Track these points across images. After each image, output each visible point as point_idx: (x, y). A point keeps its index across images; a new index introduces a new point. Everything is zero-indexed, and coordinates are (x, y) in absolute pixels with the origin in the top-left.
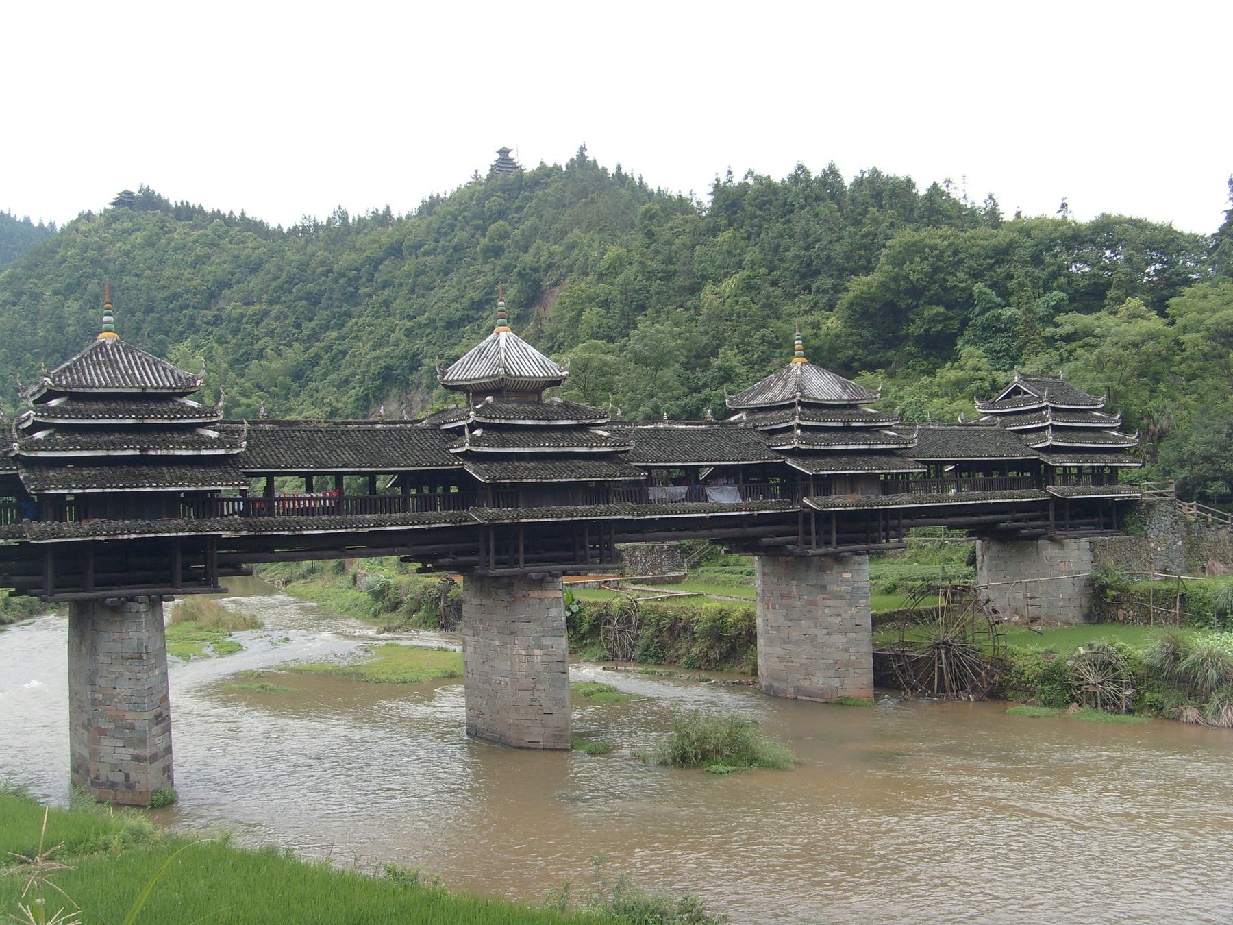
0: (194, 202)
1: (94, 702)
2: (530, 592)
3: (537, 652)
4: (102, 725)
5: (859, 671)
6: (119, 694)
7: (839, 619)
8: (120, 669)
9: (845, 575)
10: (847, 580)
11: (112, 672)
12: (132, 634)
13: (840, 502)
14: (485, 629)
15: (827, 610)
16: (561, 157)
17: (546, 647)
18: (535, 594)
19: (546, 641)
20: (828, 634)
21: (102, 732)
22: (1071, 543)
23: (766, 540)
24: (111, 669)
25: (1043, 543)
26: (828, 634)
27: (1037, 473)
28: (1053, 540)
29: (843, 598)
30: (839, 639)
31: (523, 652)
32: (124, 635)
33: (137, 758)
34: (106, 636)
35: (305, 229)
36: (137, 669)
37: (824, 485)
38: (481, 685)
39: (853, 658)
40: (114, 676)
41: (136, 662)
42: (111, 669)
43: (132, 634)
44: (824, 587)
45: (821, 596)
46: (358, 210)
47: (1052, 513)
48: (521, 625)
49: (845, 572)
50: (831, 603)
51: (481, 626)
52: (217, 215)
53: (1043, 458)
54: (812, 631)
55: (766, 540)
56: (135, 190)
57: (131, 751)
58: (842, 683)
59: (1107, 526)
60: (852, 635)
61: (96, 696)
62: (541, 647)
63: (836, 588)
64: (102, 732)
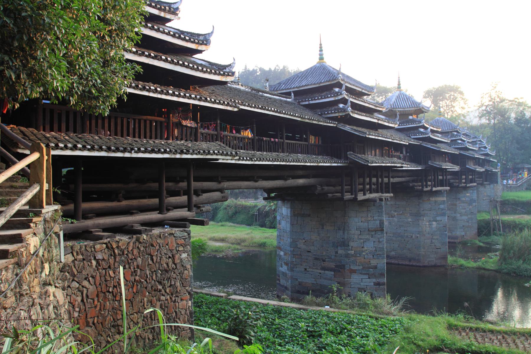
1: (347, 256)
2: (431, 198)
3: (434, 223)
4: (352, 267)
5: (472, 229)
6: (366, 250)
7: (465, 210)
8: (368, 237)
9: (467, 194)
10: (468, 196)
11: (361, 239)
12: (376, 218)
14: (401, 214)
15: (461, 207)
17: (439, 221)
18: (433, 199)
19: (438, 218)
20: (460, 216)
21: (354, 271)
22: (488, 187)
24: (360, 237)
26: (460, 216)
29: (467, 203)
30: (465, 218)
31: (428, 223)
32: (370, 219)
33: (378, 284)
34: (356, 220)
36: (379, 236)
38: (394, 239)
39: (470, 224)
40: (362, 241)
41: (379, 233)
42: (360, 237)
43: (376, 218)
44: (459, 199)
45: (458, 202)
48: (426, 212)
49: (468, 193)
50: (462, 204)
51: (396, 214)
54: (453, 215)
57: (374, 280)
58: (466, 234)
60: (470, 216)
61: (349, 252)
62: (436, 221)
63: (464, 199)
64: (354, 271)
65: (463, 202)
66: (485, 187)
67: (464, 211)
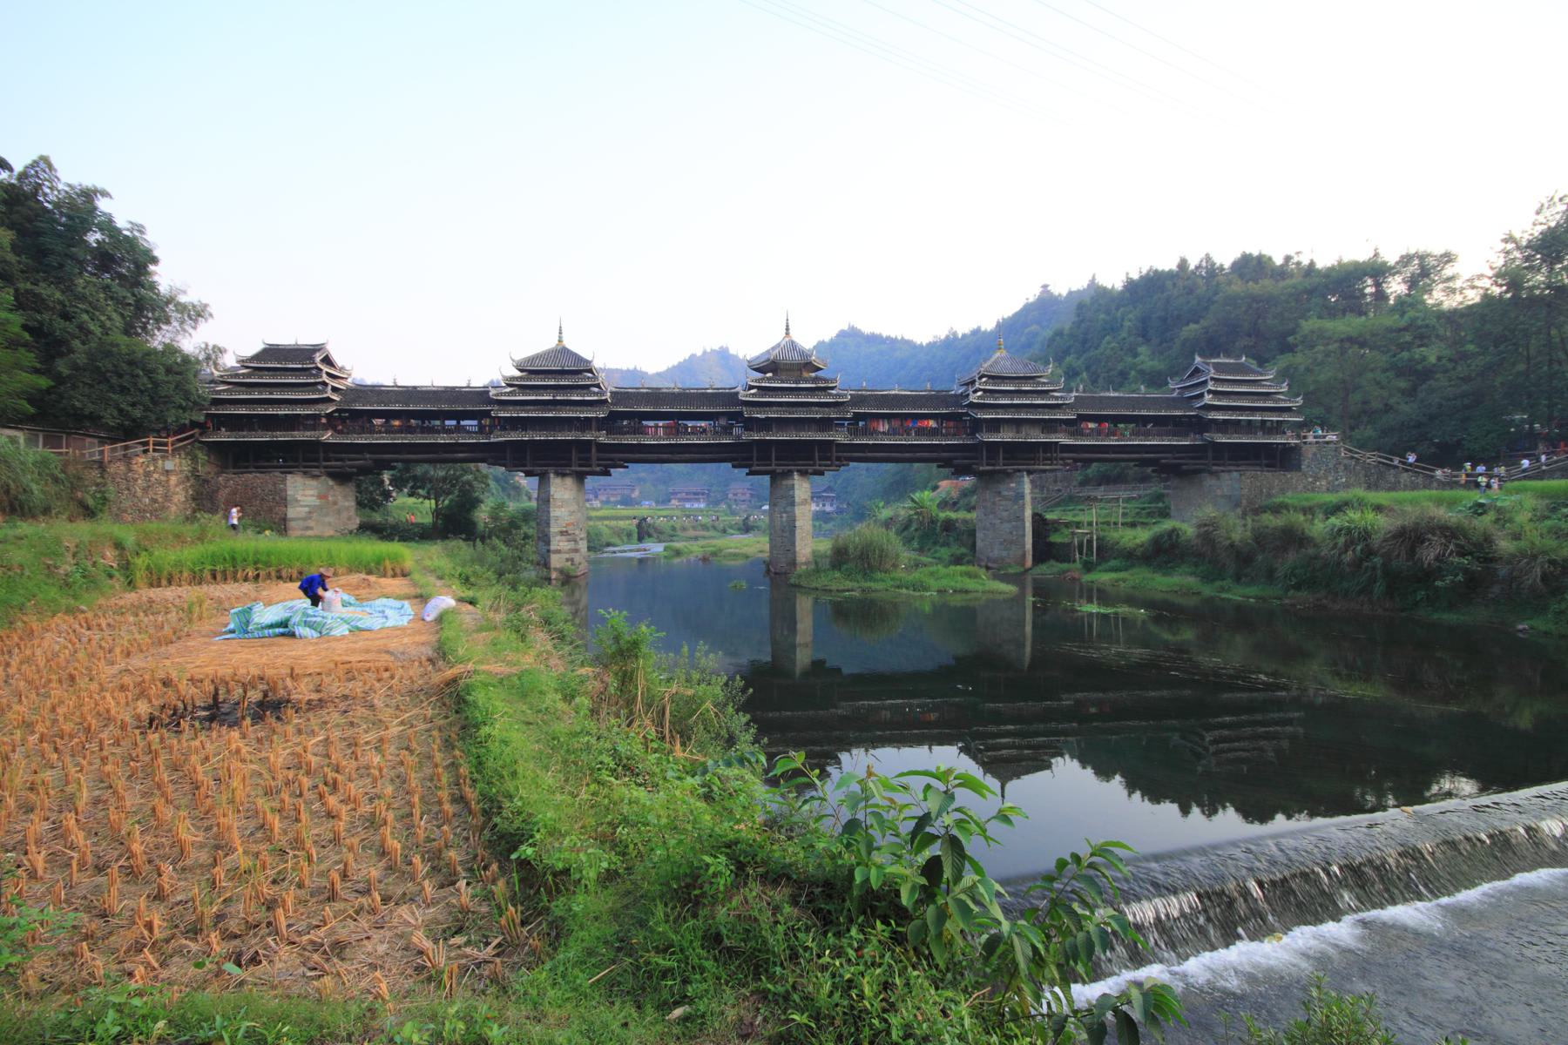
0: (877, 332)
9: (1013, 485)
13: (1006, 436)
16: (1080, 284)
23: (956, 462)
25: (1205, 475)
27: (1198, 425)
28: (1212, 473)
35: (935, 343)
37: (995, 425)
46: (963, 329)
47: (1210, 454)
52: (888, 338)
53: (1202, 413)
55: (956, 462)
56: (846, 328)
59: (1268, 466)
65: (1006, 498)
66: (1218, 478)
67: (1005, 514)
